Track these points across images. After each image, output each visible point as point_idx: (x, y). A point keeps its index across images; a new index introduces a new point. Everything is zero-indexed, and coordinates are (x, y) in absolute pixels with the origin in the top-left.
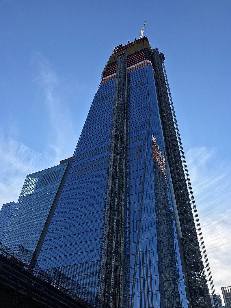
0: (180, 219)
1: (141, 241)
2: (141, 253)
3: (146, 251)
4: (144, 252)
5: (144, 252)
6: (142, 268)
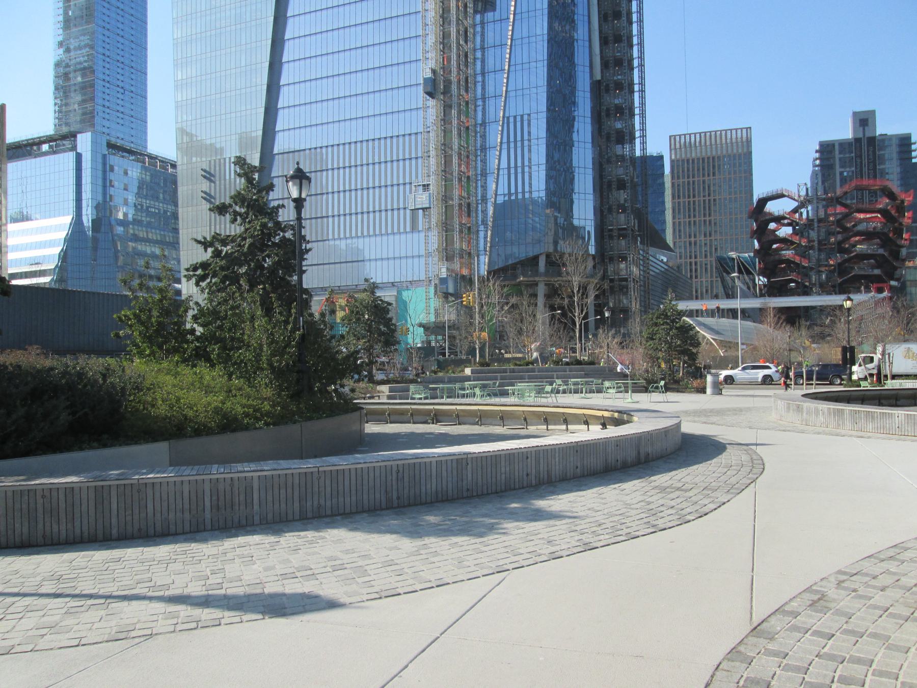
0: (600, 32)
1: (512, 94)
2: (512, 120)
3: (522, 116)
4: (519, 119)
5: (519, 119)
6: (512, 151)
